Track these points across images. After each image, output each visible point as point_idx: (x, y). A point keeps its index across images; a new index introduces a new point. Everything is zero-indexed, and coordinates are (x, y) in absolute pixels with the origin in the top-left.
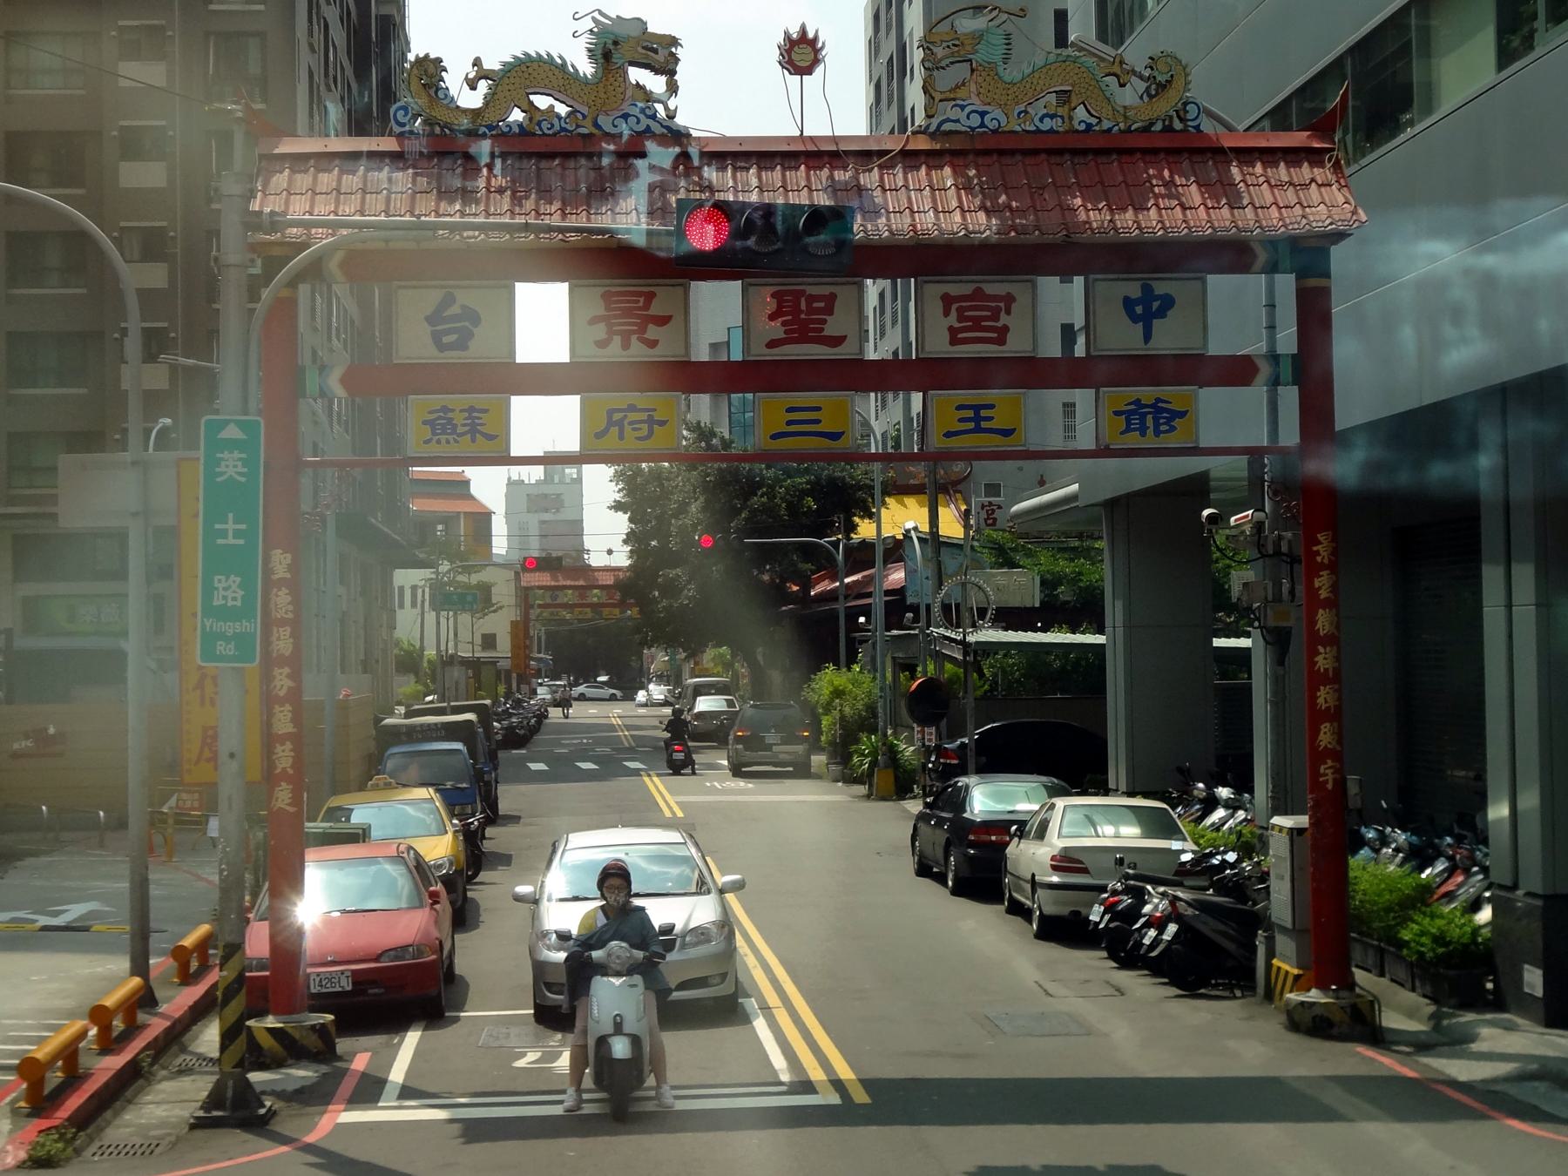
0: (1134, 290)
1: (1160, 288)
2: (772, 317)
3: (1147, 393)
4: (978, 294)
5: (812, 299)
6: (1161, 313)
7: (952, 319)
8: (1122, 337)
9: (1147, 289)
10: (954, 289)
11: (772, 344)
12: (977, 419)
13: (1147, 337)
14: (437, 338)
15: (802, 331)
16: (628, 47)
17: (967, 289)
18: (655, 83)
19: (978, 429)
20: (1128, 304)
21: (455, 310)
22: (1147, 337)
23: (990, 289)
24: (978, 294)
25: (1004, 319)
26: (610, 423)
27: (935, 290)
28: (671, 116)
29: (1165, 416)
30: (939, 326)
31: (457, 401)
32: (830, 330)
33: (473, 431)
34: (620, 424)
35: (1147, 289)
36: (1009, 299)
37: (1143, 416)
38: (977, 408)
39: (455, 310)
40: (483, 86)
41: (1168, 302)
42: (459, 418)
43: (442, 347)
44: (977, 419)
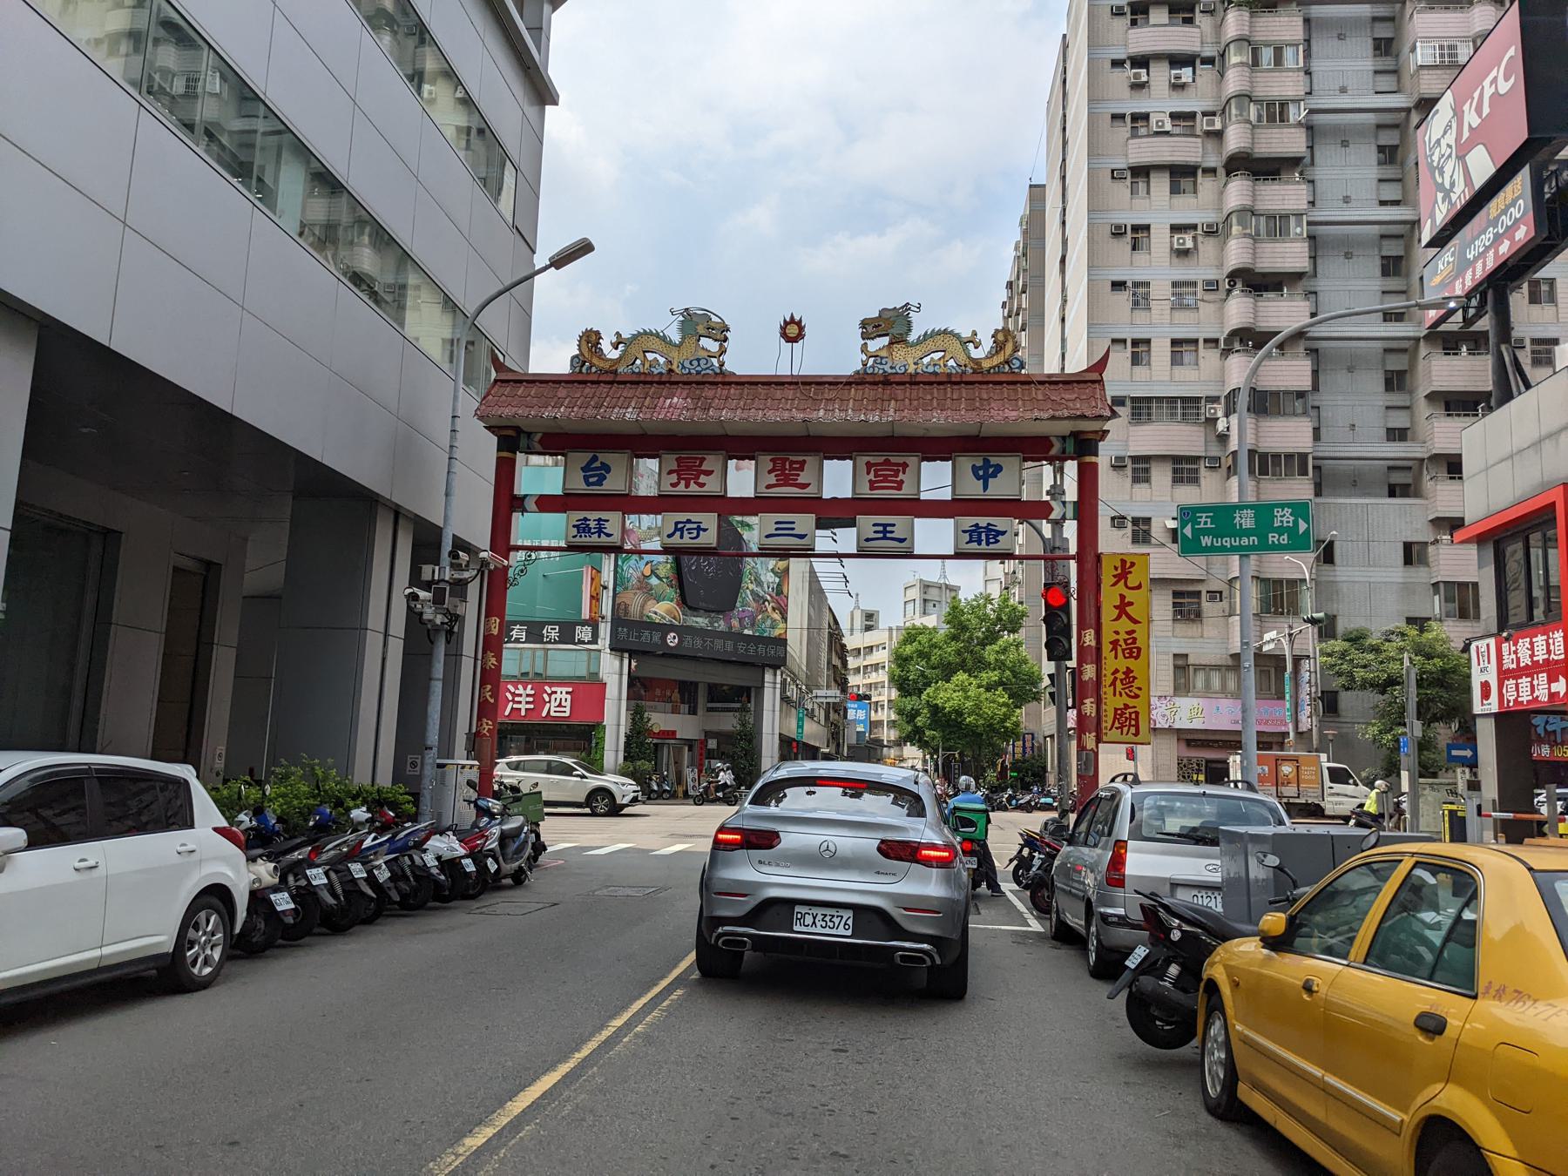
0: (980, 463)
1: (994, 460)
2: (770, 472)
3: (983, 521)
4: (887, 462)
5: (792, 462)
6: (994, 475)
7: (872, 476)
8: (973, 488)
9: (986, 461)
10: (872, 460)
11: (768, 487)
12: (885, 532)
13: (985, 488)
14: (586, 479)
15: (785, 481)
16: (698, 324)
17: (881, 460)
18: (711, 345)
19: (885, 538)
20: (975, 469)
21: (597, 464)
22: (985, 488)
23: (893, 460)
24: (887, 462)
25: (901, 476)
26: (676, 529)
27: (863, 460)
28: (722, 365)
29: (994, 534)
30: (865, 480)
31: (593, 516)
32: (801, 480)
33: (600, 531)
34: (681, 530)
35: (986, 461)
36: (905, 465)
37: (980, 534)
38: (885, 526)
39: (597, 464)
40: (621, 347)
41: (999, 469)
42: (592, 524)
43: (588, 484)
44: (885, 532)
